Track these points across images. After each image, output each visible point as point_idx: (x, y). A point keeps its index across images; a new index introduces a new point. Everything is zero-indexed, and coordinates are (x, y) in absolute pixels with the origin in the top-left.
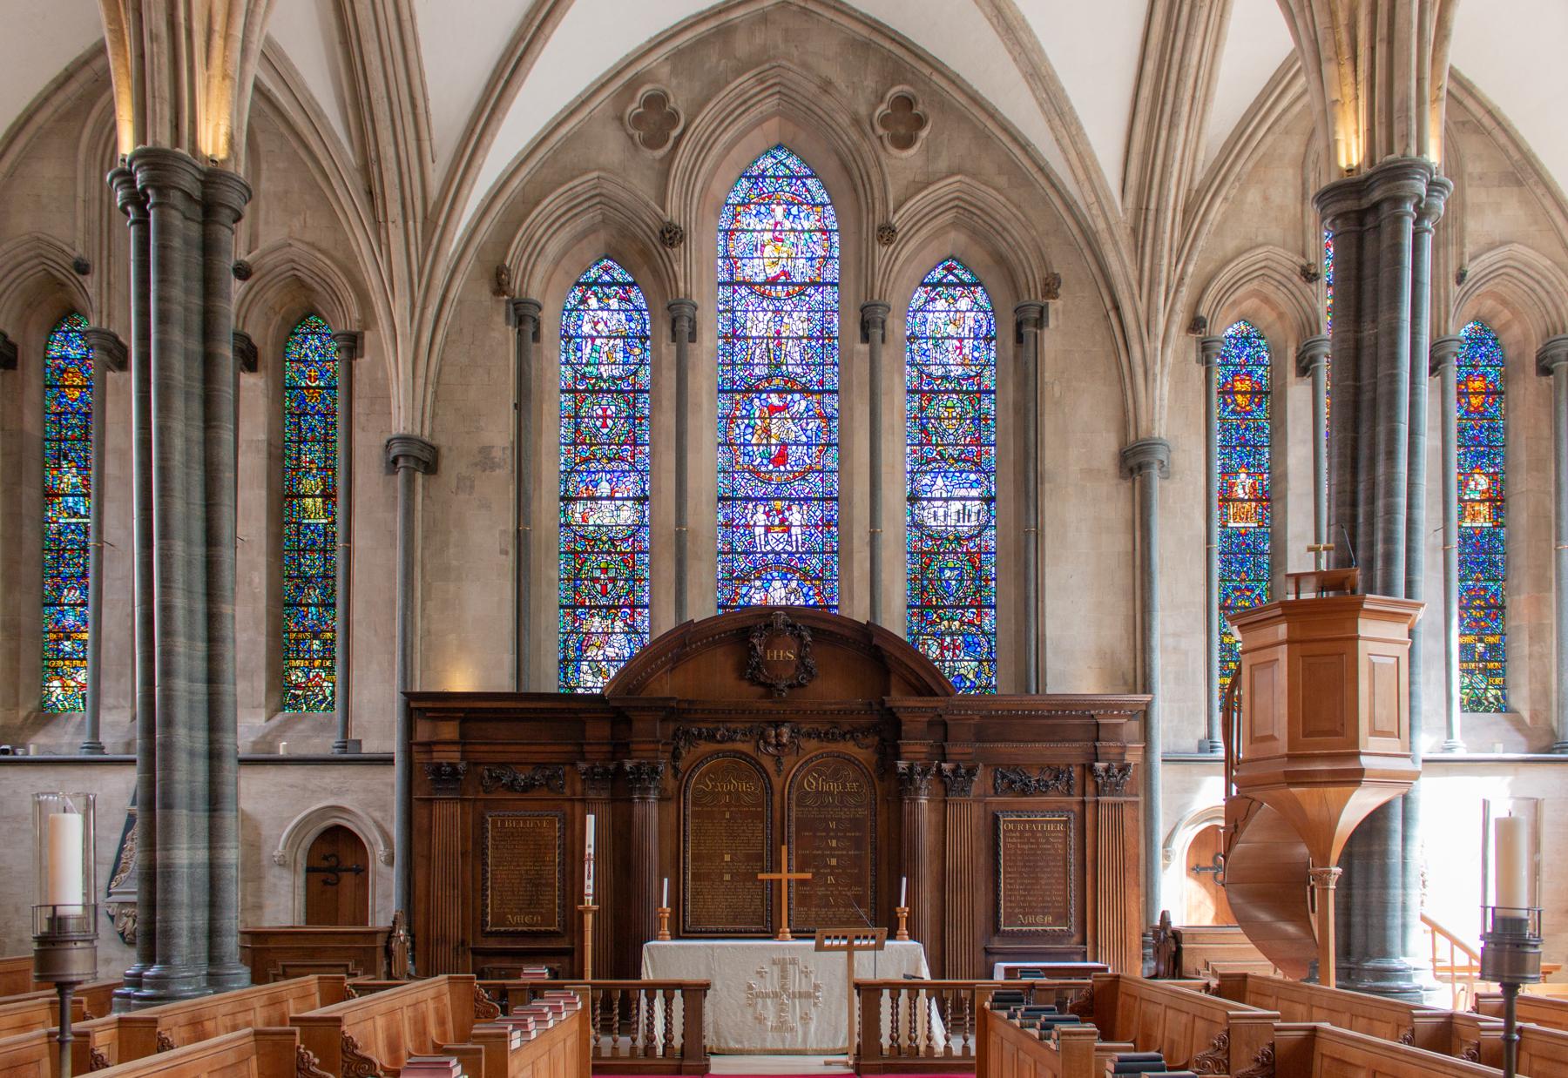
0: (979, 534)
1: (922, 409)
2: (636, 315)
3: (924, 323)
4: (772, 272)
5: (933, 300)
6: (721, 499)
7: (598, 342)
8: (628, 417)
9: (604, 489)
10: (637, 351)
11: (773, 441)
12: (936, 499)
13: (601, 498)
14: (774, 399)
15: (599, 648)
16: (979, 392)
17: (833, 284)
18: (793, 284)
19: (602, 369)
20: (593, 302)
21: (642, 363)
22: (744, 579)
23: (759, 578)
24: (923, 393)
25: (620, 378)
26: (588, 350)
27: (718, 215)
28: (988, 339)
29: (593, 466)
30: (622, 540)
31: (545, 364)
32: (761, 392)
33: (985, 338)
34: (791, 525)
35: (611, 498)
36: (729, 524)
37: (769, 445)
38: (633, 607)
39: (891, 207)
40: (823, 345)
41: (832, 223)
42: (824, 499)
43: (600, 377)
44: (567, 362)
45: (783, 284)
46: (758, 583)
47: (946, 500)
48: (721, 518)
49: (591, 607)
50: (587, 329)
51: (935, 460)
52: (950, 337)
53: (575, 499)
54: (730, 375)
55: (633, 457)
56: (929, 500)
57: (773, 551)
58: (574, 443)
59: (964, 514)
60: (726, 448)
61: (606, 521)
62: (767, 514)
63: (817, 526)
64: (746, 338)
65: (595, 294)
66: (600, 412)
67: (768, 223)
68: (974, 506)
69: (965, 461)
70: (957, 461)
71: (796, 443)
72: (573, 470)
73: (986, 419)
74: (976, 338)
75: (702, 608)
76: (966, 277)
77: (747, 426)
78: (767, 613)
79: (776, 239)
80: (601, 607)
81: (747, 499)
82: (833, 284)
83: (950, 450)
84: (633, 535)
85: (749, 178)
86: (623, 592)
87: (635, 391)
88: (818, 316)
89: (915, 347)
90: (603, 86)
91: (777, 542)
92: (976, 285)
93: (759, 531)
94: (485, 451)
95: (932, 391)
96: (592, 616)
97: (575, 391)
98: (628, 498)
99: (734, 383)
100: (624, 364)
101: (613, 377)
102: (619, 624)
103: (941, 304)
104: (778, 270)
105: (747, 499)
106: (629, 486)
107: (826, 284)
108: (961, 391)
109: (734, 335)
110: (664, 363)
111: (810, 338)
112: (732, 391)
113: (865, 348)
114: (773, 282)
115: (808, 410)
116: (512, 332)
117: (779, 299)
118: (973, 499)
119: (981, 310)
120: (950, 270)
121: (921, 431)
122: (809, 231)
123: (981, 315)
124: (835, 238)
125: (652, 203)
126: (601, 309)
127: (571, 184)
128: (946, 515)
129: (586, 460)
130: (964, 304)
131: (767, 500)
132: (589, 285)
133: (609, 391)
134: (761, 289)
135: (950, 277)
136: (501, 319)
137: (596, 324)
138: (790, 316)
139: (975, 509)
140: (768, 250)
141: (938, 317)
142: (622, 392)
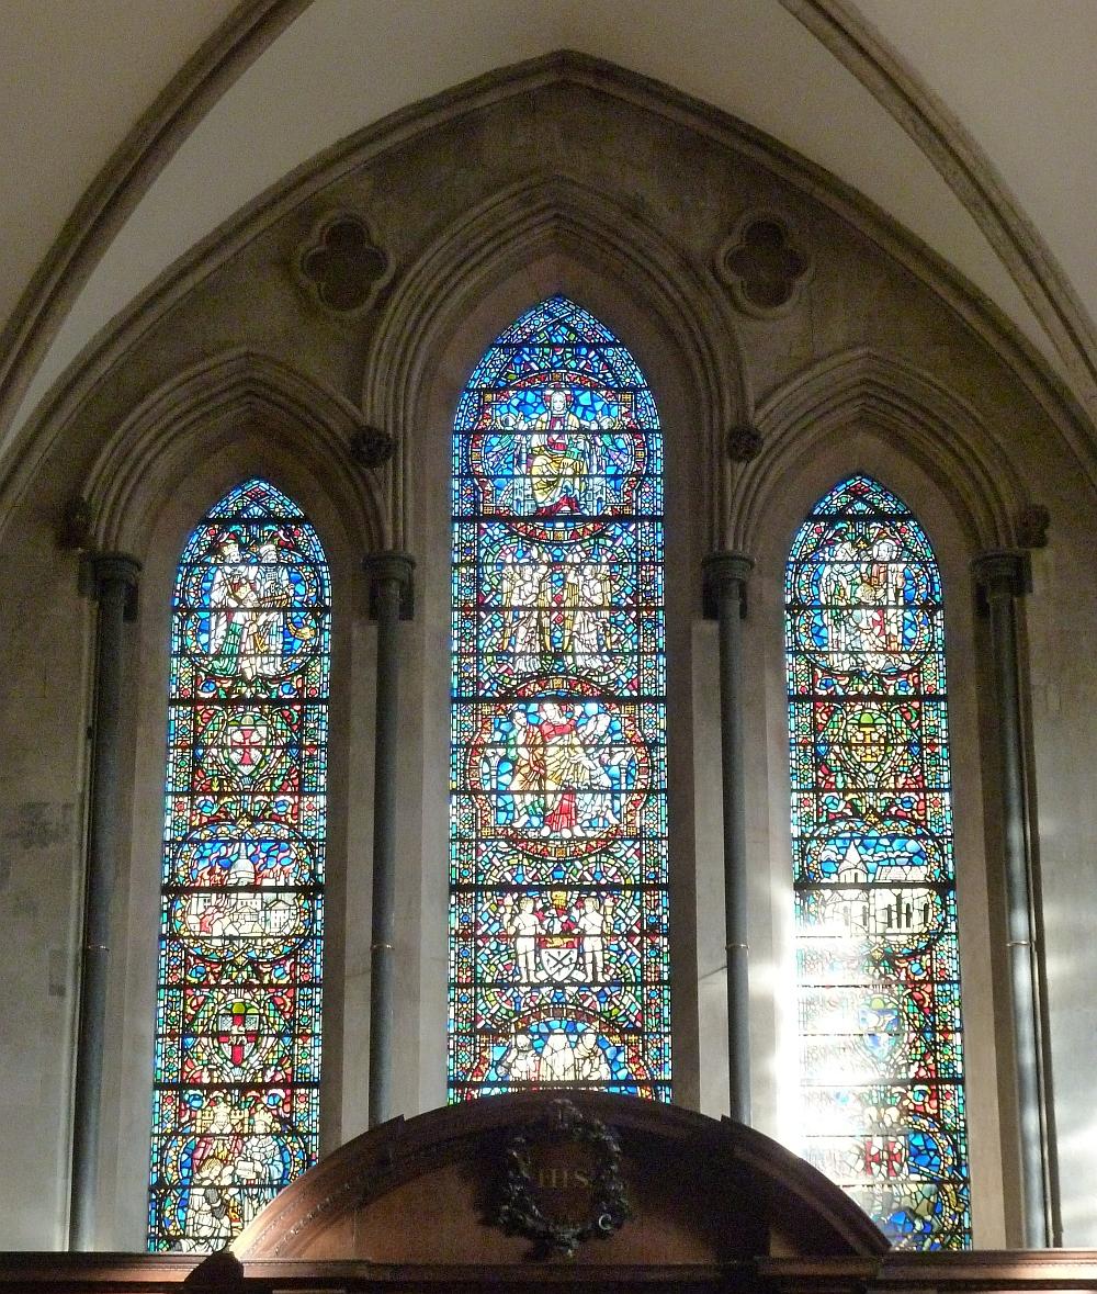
0: (929, 947)
1: (816, 728)
2: (307, 571)
3: (815, 582)
4: (545, 499)
5: (831, 543)
6: (456, 888)
7: (239, 618)
8: (287, 746)
9: (243, 871)
10: (307, 633)
11: (551, 785)
12: (845, 886)
13: (236, 889)
14: (551, 711)
15: (225, 1162)
16: (917, 697)
17: (653, 519)
18: (585, 519)
19: (245, 664)
20: (232, 551)
21: (315, 652)
22: (496, 1032)
23: (525, 1031)
24: (815, 698)
25: (277, 679)
26: (221, 631)
27: (451, 406)
28: (929, 608)
29: (224, 830)
30: (274, 963)
31: (143, 658)
32: (527, 700)
33: (924, 606)
34: (583, 934)
35: (253, 888)
36: (468, 933)
37: (541, 792)
38: (290, 1085)
39: (751, 399)
40: (638, 621)
41: (650, 418)
42: (640, 888)
43: (238, 678)
44: (183, 652)
45: (566, 519)
46: (523, 1040)
47: (866, 887)
48: (455, 923)
49: (211, 1087)
50: (218, 595)
51: (844, 817)
52: (860, 605)
53: (189, 891)
54: (472, 672)
55: (296, 815)
56: (834, 887)
57: (550, 982)
58: (192, 793)
59: (901, 912)
60: (464, 800)
61: (246, 930)
62: (539, 913)
63: (630, 935)
64: (500, 609)
65: (236, 538)
66: (238, 737)
67: (541, 420)
68: (917, 898)
69: (896, 818)
70: (882, 819)
71: (590, 790)
72: (186, 840)
73: (932, 745)
74: (908, 606)
75: (421, 1090)
76: (888, 505)
77: (504, 759)
78: (536, 1101)
79: (553, 444)
80: (229, 1087)
81: (503, 888)
82: (653, 519)
83: (870, 799)
84: (293, 954)
85: (505, 347)
86: (273, 1059)
87: (301, 701)
88: (629, 570)
89: (801, 621)
90: (259, 213)
91: (556, 964)
92: (904, 518)
93: (525, 945)
94: (33, 810)
95: (832, 698)
96: (214, 1102)
97: (194, 701)
98: (286, 889)
99: (478, 684)
100: (283, 655)
101: (265, 679)
102: (263, 1120)
103: (844, 551)
104: (556, 495)
105: (503, 888)
106: (287, 868)
107: (642, 518)
108: (885, 698)
109: (481, 606)
110: (356, 657)
111: (615, 608)
112: (476, 699)
113: (711, 628)
114: (549, 515)
115: (610, 731)
116: (87, 607)
117: (559, 544)
118: (914, 885)
119: (917, 559)
120: (857, 494)
121: (817, 767)
122: (610, 432)
123: (916, 568)
124: (657, 443)
125: (344, 400)
126: (245, 562)
127: (200, 367)
128: (866, 915)
129: (214, 821)
130: (883, 550)
131: (541, 889)
132: (225, 523)
133: (255, 701)
134: (531, 527)
135: (860, 506)
136: (69, 586)
137: (236, 587)
138: (579, 571)
139: (919, 905)
140: (539, 461)
141: (839, 569)
142: (279, 702)
